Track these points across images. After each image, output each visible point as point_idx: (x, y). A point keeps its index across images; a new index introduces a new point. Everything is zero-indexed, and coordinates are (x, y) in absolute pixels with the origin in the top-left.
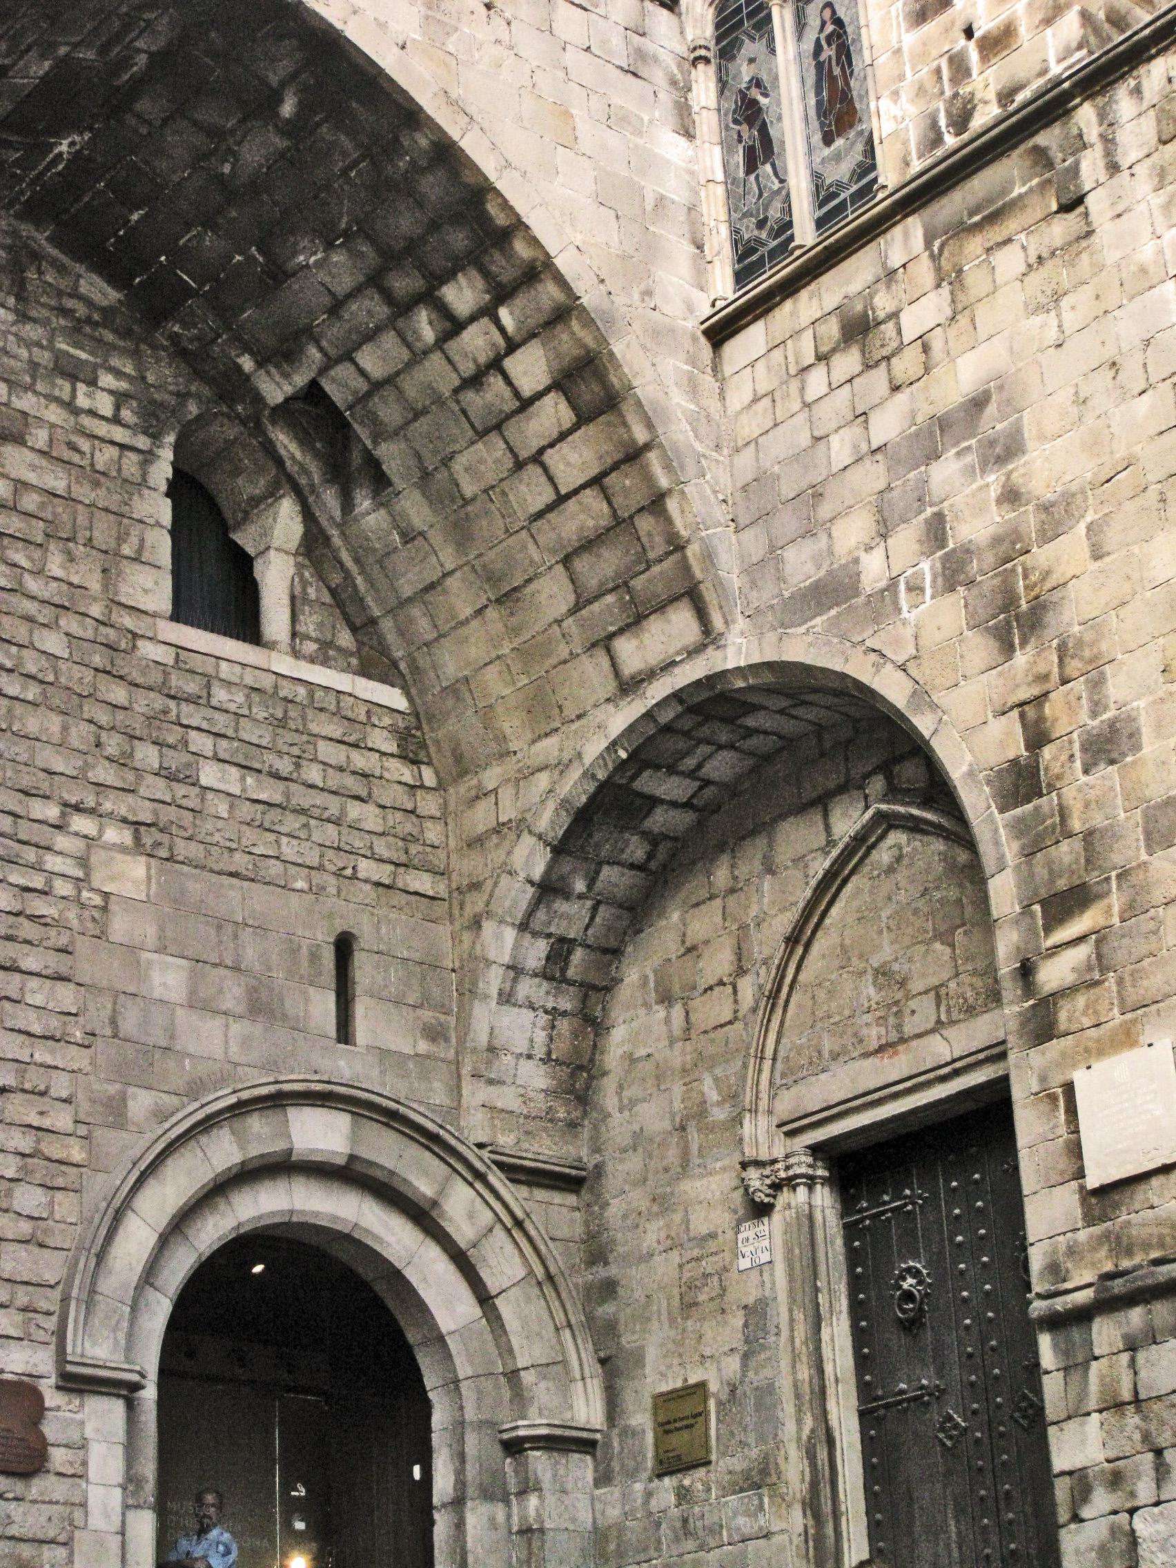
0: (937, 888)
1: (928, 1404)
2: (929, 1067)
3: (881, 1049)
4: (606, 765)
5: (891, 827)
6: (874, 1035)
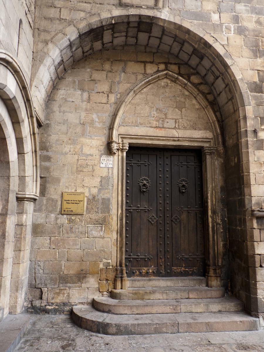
0: (178, 97)
1: (146, 212)
2: (171, 136)
3: (156, 127)
4: (107, 21)
5: (166, 77)
6: (155, 123)
